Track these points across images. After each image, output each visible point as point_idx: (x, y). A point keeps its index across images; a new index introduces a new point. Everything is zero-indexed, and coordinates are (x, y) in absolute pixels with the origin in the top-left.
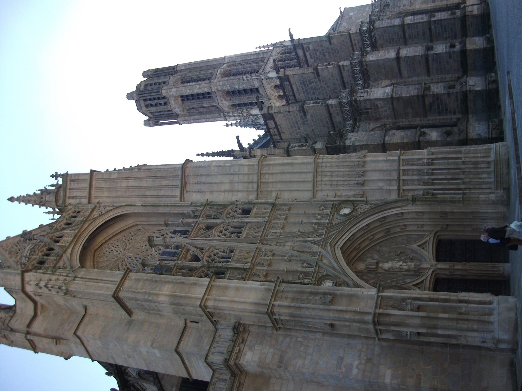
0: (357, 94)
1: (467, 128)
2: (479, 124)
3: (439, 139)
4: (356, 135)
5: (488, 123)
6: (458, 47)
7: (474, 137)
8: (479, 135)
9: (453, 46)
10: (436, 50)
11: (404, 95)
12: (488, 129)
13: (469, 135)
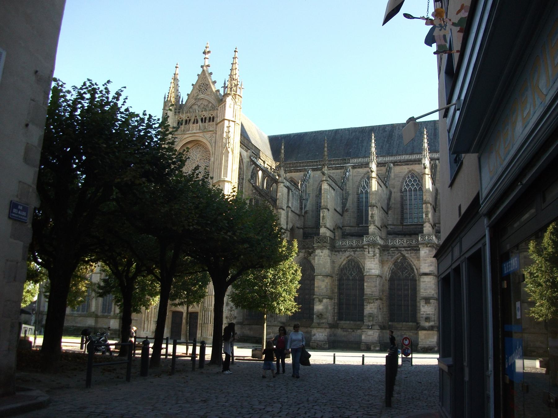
0: (371, 248)
1: (322, 328)
2: (325, 335)
3: (315, 310)
4: (325, 256)
5: (326, 341)
6: (427, 324)
7: (312, 332)
8: (315, 335)
9: (427, 319)
10: (426, 306)
11: (365, 284)
12: (319, 341)
13: (315, 329)
